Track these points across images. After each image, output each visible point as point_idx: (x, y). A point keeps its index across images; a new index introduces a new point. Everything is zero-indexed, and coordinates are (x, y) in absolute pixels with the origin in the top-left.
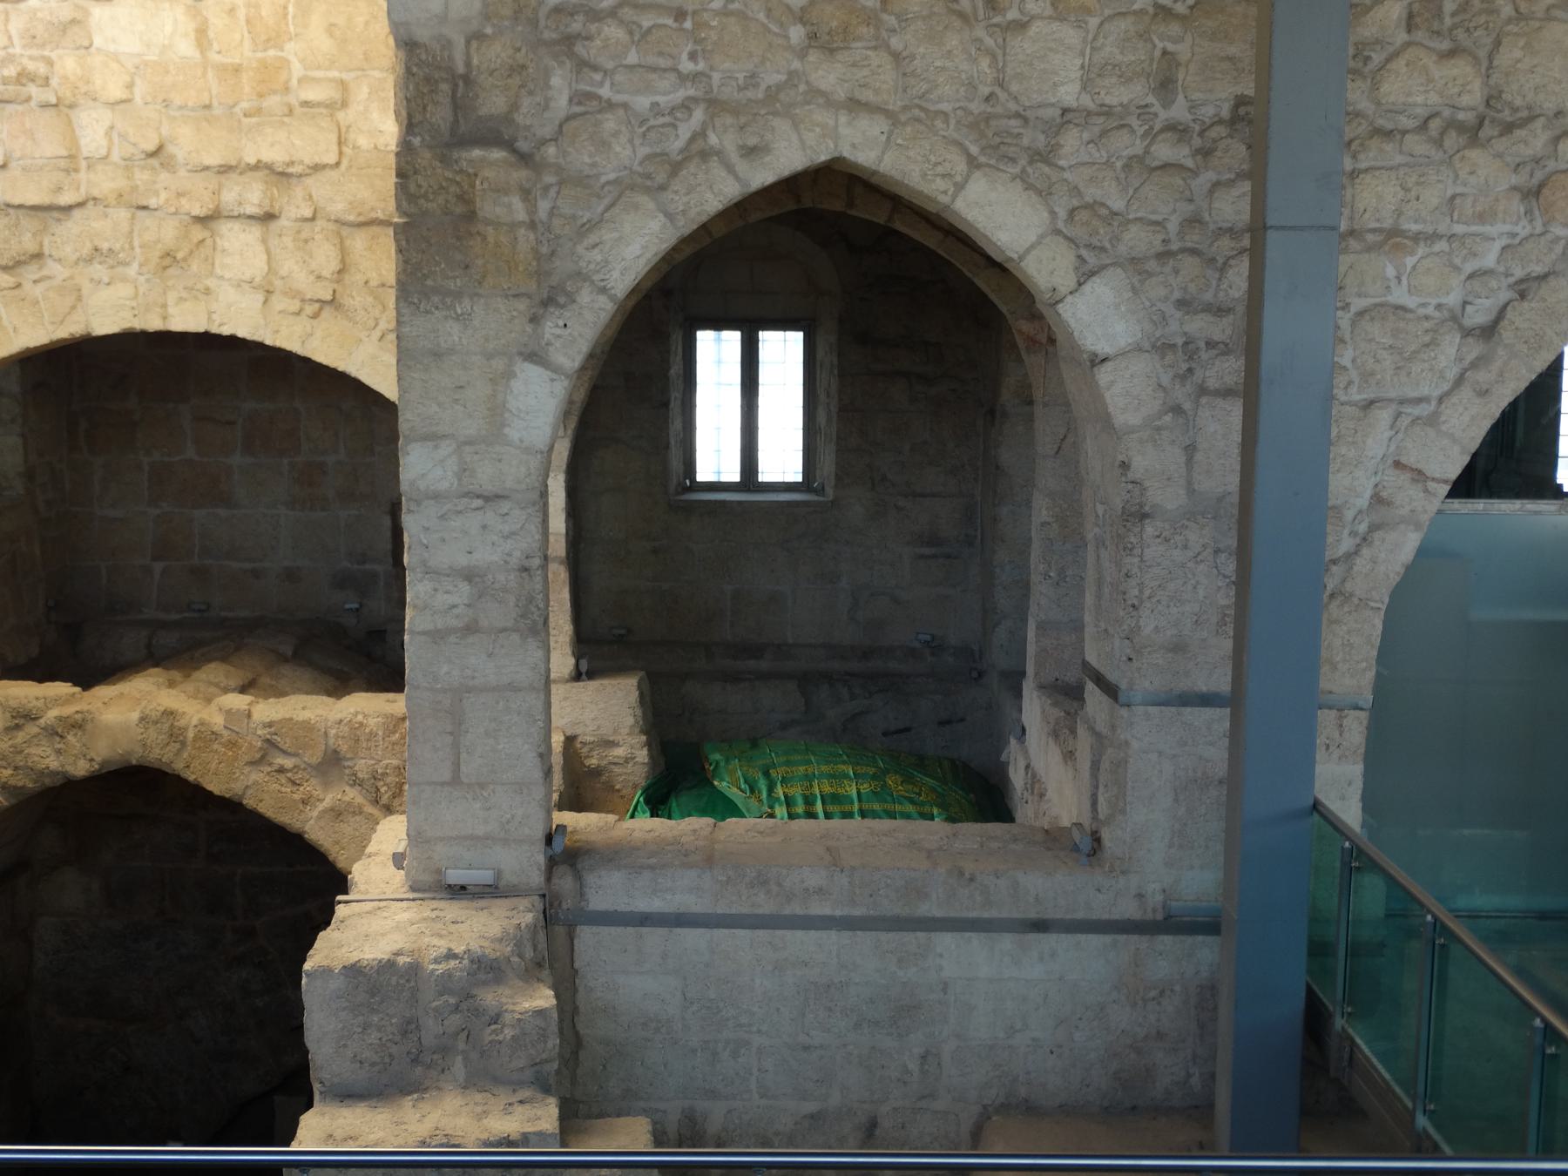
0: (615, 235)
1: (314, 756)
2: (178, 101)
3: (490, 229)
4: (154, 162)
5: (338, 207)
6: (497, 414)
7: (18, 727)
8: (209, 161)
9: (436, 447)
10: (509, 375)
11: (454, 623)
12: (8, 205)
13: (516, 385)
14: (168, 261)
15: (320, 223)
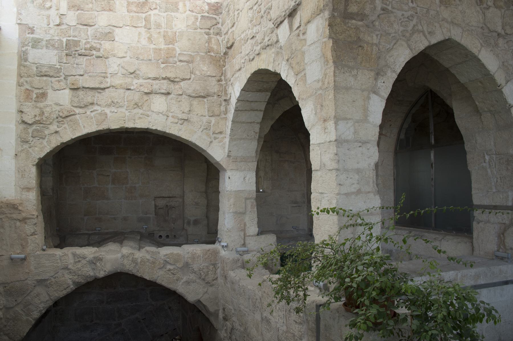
0: (397, 53)
1: (179, 265)
2: (141, 58)
3: (365, 45)
4: (132, 76)
5: (190, 92)
6: (366, 110)
7: (79, 261)
8: (150, 76)
9: (347, 123)
10: (369, 98)
11: (353, 190)
12: (84, 87)
13: (371, 102)
14: (135, 106)
15: (184, 96)
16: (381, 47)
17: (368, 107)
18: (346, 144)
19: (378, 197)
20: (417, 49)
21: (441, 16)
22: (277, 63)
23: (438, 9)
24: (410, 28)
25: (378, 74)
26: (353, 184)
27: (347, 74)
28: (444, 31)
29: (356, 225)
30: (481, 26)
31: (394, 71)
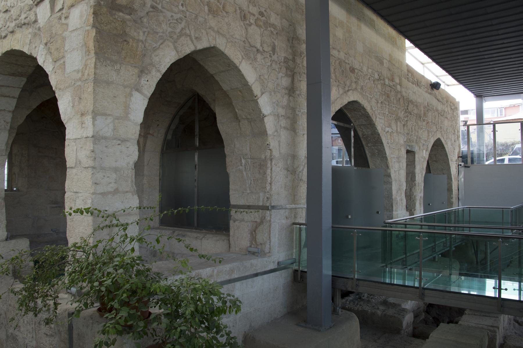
0: (163, 53)
3: (131, 40)
6: (127, 107)
9: (106, 119)
10: (131, 95)
13: (133, 99)
16: (147, 44)
17: (129, 105)
18: (104, 140)
19: (136, 197)
20: (183, 52)
21: (208, 24)
22: (34, 46)
23: (206, 17)
24: (178, 30)
25: (142, 72)
26: (110, 183)
27: (110, 68)
28: (211, 38)
29: (113, 225)
30: (244, 39)
31: (159, 71)
